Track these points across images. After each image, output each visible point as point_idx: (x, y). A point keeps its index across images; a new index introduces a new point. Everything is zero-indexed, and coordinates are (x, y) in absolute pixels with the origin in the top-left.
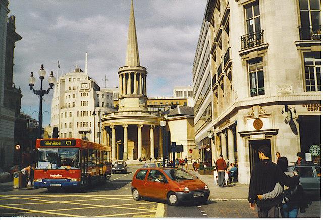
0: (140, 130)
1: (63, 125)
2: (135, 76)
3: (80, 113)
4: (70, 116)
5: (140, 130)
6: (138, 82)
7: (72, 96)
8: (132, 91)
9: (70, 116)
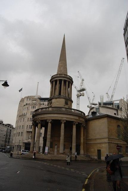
0: (63, 126)
1: (19, 127)
2: (63, 82)
3: (29, 119)
4: (24, 121)
5: (63, 126)
6: (65, 87)
7: (26, 108)
8: (60, 94)
9: (24, 121)
